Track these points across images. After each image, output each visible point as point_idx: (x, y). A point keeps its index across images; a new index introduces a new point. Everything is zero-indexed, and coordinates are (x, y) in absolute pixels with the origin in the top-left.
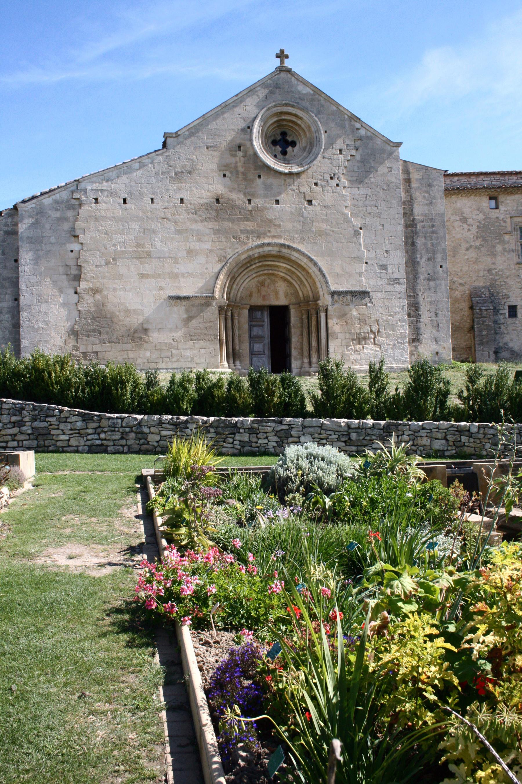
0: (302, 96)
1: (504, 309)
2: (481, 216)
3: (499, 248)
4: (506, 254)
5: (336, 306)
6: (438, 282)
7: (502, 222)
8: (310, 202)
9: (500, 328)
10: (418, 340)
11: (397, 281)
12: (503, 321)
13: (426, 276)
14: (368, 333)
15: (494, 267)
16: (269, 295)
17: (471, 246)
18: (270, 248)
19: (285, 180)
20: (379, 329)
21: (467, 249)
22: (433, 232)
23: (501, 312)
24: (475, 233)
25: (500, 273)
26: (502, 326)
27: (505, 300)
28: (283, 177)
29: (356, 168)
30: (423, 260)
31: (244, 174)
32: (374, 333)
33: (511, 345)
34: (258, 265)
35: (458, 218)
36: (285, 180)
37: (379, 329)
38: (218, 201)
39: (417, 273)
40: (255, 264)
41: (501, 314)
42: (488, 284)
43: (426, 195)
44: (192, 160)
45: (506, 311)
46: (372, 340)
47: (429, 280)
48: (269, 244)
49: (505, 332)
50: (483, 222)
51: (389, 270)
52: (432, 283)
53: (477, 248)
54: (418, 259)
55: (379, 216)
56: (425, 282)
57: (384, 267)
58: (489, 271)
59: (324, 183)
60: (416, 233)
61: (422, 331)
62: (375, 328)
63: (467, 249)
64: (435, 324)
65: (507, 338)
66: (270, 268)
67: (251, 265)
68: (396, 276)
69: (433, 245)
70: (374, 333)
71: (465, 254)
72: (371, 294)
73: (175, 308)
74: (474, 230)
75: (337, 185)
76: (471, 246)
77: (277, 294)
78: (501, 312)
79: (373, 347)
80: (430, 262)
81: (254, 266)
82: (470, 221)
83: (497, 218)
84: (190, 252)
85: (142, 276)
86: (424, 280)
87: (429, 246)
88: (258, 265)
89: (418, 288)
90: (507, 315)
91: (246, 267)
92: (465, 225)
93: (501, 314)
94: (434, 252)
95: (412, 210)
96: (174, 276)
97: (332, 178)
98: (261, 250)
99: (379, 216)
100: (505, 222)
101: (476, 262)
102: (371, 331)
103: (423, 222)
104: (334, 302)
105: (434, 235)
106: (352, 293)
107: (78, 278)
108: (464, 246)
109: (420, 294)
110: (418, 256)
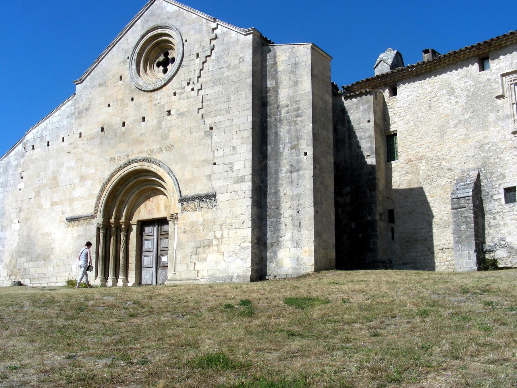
0: (169, 15)
1: (499, 193)
2: (471, 83)
3: (492, 117)
4: (500, 122)
5: (185, 214)
6: (301, 172)
7: (493, 84)
8: (169, 112)
9: (495, 218)
10: (278, 243)
11: (242, 180)
12: (498, 209)
13: (288, 167)
14: (212, 240)
15: (487, 141)
16: (153, 208)
17: (460, 121)
18: (136, 164)
19: (151, 97)
20: (222, 234)
21: (456, 126)
22: (298, 116)
23: (495, 197)
24: (464, 104)
25: (494, 148)
26: (498, 217)
27: (500, 182)
28: (149, 94)
29: (211, 68)
30: (286, 150)
31: (122, 100)
32: (218, 239)
33: (509, 240)
34: (134, 181)
35: (445, 92)
36: (151, 97)
37: (222, 234)
38: (102, 129)
39: (279, 166)
40: (132, 180)
41: (496, 200)
42: (480, 164)
43: (292, 76)
44: (89, 99)
45: (502, 196)
46: (216, 248)
47: (291, 172)
48: (134, 161)
49: (502, 223)
50: (472, 90)
51: (236, 167)
52: (295, 175)
53: (467, 122)
54: (281, 150)
55: (228, 111)
56: (289, 174)
57: (231, 166)
58: (481, 147)
59: (180, 91)
60: (280, 121)
61: (282, 232)
62: (219, 234)
63: (456, 126)
64: (297, 223)
65: (504, 231)
66: (148, 183)
67: (129, 183)
68: (242, 173)
69: (297, 131)
70: (218, 239)
71: (454, 132)
72: (218, 196)
73: (70, 229)
74: (462, 101)
75: (193, 90)
76: (460, 121)
77: (158, 208)
78: (495, 197)
79: (217, 255)
80: (293, 151)
81: (131, 184)
82: (458, 92)
83: (488, 80)
84: (83, 178)
85: (54, 204)
86: (286, 173)
87: (293, 133)
88: (134, 181)
89: (280, 182)
90: (503, 201)
91: (125, 185)
92: (452, 98)
93: (496, 200)
94: (298, 138)
95: (277, 96)
96: (71, 201)
97: (188, 84)
98: (129, 167)
99: (228, 111)
100: (497, 82)
101: (467, 137)
102: (215, 237)
103: (287, 106)
104: (183, 209)
105: (299, 118)
106: (200, 198)
107: (20, 210)
108: (452, 123)
109: (281, 189)
110: (281, 146)
